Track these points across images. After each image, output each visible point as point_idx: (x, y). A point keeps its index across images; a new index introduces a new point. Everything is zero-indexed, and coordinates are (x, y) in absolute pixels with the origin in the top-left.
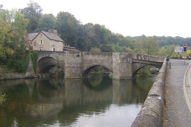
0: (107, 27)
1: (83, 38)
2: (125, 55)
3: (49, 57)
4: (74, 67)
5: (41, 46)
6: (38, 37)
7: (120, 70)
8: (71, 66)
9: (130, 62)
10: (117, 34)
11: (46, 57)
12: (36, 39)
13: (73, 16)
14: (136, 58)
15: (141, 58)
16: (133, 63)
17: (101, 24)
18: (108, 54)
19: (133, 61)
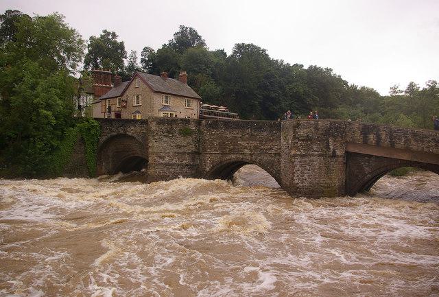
0: (336, 72)
1: (273, 95)
2: (317, 129)
3: (125, 136)
4: (174, 164)
5: (137, 109)
6: (131, 88)
7: (296, 181)
8: (161, 161)
9: (338, 153)
10: (363, 88)
11: (119, 136)
12: (127, 93)
13: (264, 51)
14: (358, 136)
15: (378, 136)
16: (349, 155)
17: (322, 65)
18: (271, 127)
19: (352, 149)
